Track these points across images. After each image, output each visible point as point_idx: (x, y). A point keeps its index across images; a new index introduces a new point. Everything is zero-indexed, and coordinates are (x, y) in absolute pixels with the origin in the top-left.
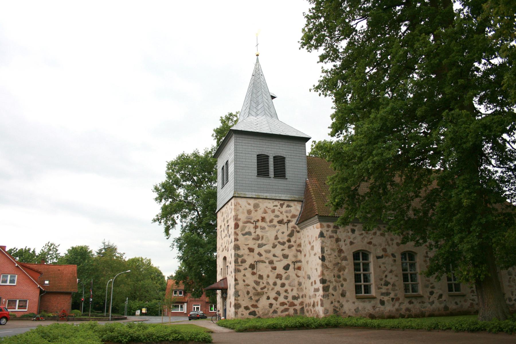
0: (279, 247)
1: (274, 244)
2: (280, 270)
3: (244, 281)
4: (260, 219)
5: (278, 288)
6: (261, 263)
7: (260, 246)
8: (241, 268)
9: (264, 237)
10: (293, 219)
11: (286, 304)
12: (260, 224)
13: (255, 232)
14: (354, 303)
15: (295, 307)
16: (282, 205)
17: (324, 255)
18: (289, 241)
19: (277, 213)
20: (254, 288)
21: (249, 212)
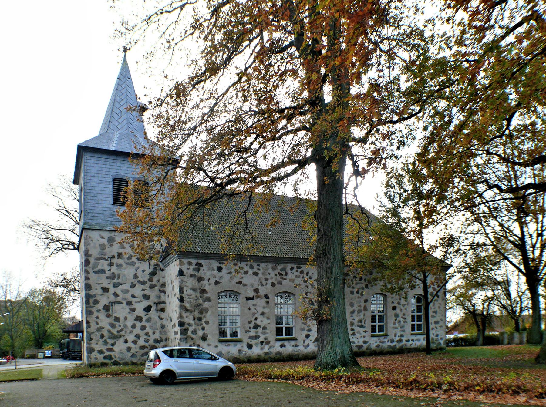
0: (139, 287)
1: (132, 283)
3: (97, 323)
4: (116, 255)
5: (137, 331)
6: (117, 305)
7: (116, 285)
8: (94, 310)
9: (121, 276)
11: (147, 348)
12: (115, 261)
13: (110, 270)
14: (216, 347)
17: (183, 295)
20: (109, 331)
21: (103, 247)
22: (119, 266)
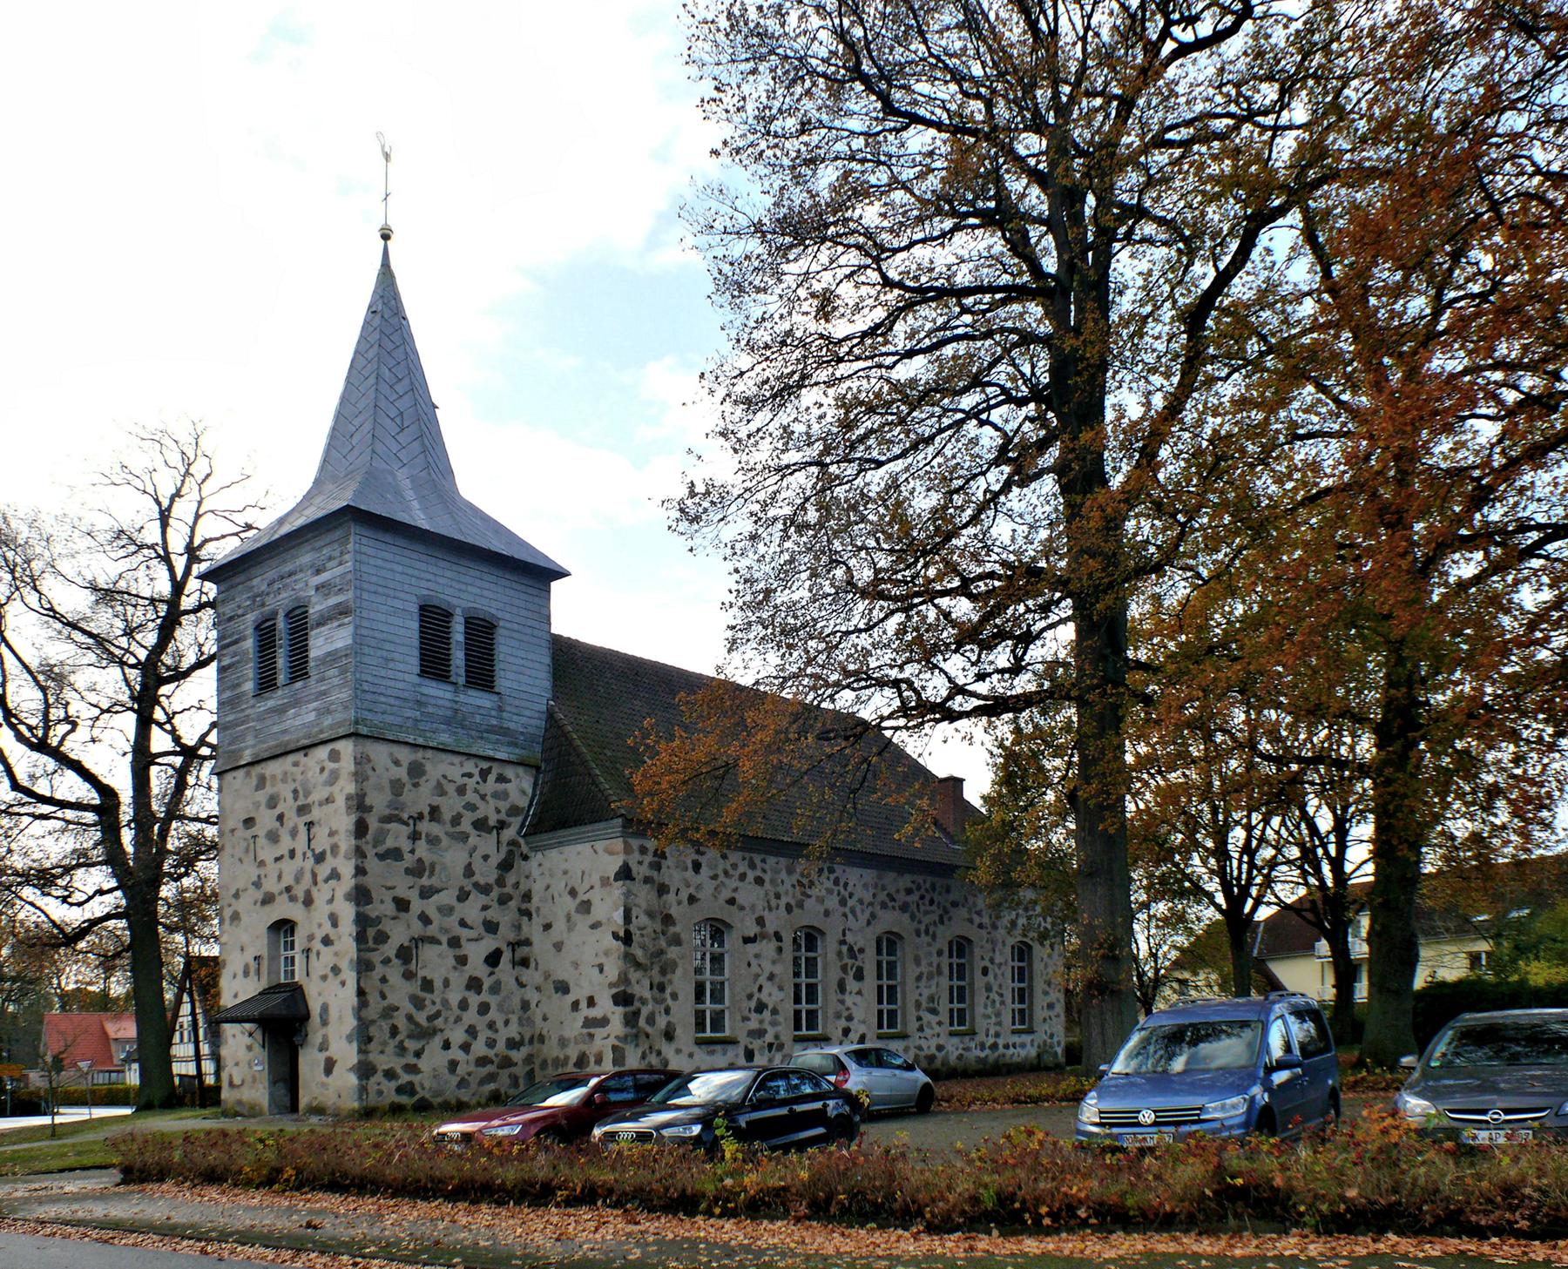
0: (477, 900)
2: (477, 967)
5: (471, 1017)
6: (427, 946)
7: (426, 893)
9: (438, 868)
10: (512, 819)
15: (513, 1070)
16: (484, 774)
18: (501, 882)
19: (471, 796)
22: (433, 841)
